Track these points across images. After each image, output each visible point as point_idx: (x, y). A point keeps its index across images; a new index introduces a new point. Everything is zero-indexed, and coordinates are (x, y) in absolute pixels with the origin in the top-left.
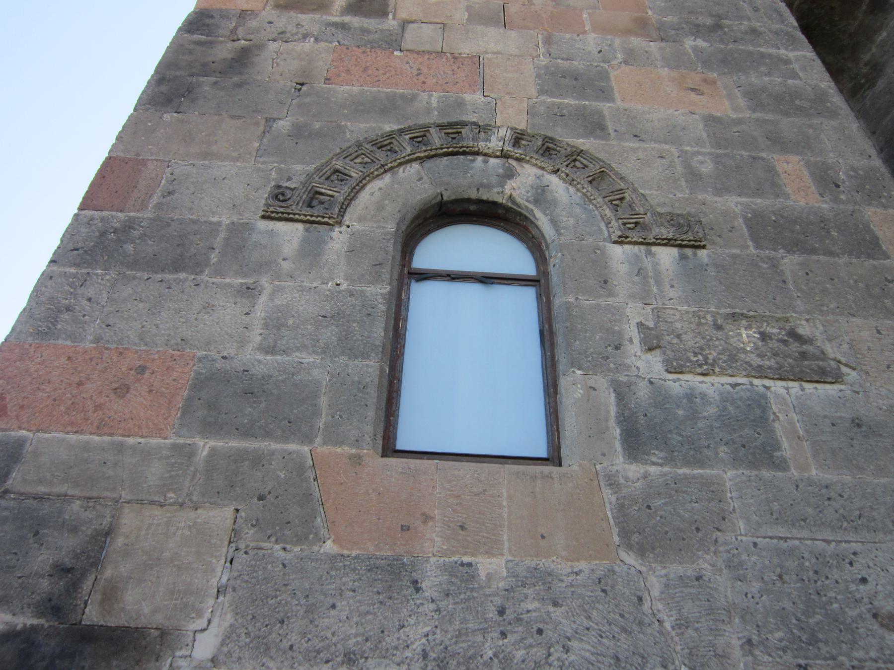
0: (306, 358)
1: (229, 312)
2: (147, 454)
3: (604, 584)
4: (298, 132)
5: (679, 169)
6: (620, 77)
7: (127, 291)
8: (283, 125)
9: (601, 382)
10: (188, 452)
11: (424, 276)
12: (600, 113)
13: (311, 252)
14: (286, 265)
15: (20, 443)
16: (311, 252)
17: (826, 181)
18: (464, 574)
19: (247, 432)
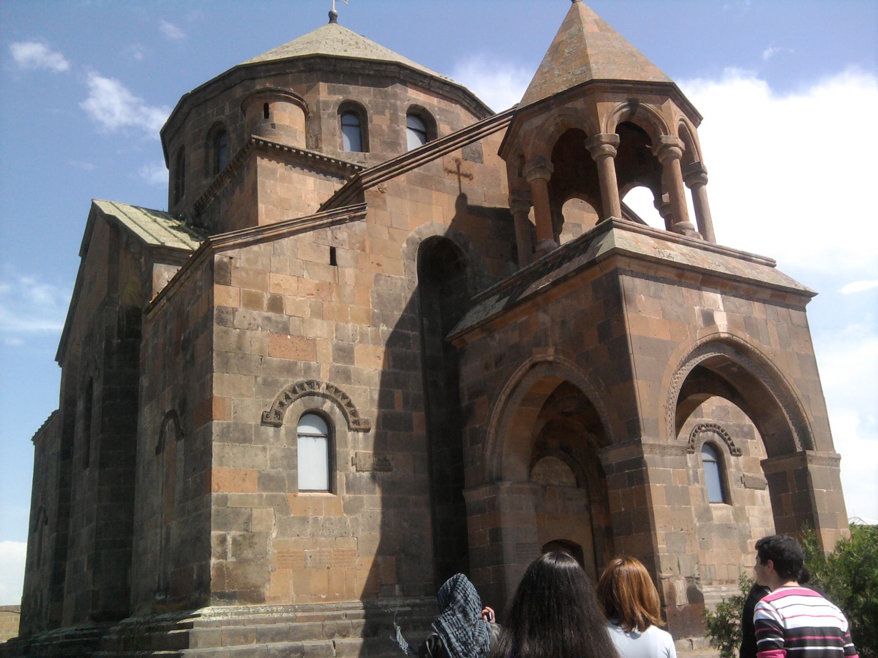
0: (281, 470)
1: (261, 455)
2: (254, 497)
3: (340, 520)
4: (266, 383)
5: (369, 397)
6: (358, 349)
7: (235, 451)
8: (259, 379)
9: (343, 474)
10: (261, 496)
11: (300, 436)
12: (349, 371)
13: (277, 435)
14: (271, 440)
15: (226, 496)
16: (277, 435)
17: (406, 402)
18: (316, 520)
19: (272, 491)
